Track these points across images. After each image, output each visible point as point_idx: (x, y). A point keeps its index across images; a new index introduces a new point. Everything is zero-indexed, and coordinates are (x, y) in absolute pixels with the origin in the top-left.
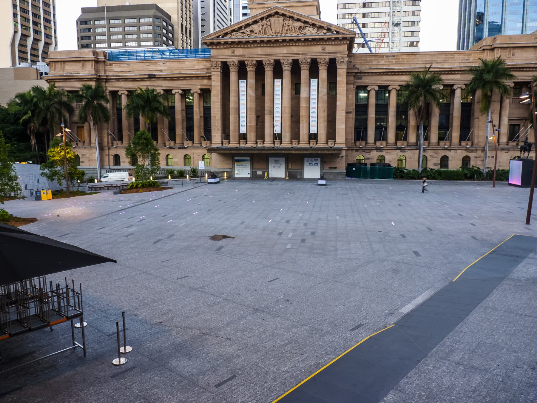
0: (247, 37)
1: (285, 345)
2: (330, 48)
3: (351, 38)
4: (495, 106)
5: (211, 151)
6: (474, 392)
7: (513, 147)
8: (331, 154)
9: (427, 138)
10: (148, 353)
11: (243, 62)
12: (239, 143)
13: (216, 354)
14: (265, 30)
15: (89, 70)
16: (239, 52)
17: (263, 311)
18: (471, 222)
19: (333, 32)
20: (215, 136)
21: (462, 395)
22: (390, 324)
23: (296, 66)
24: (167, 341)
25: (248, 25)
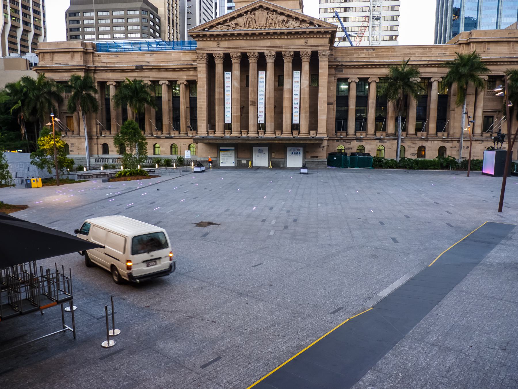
0: (232, 30)
1: (269, 327)
2: (312, 41)
3: (333, 31)
4: (470, 99)
5: (197, 140)
6: (448, 371)
7: (487, 138)
8: (313, 144)
9: (405, 129)
10: (136, 335)
12: (225, 133)
13: (201, 337)
14: (249, 23)
15: (77, 61)
16: (224, 44)
17: (247, 295)
18: (447, 210)
19: (315, 26)
20: (201, 126)
21: (437, 375)
22: (369, 308)
23: (279, 59)
24: (155, 324)
25: (233, 18)
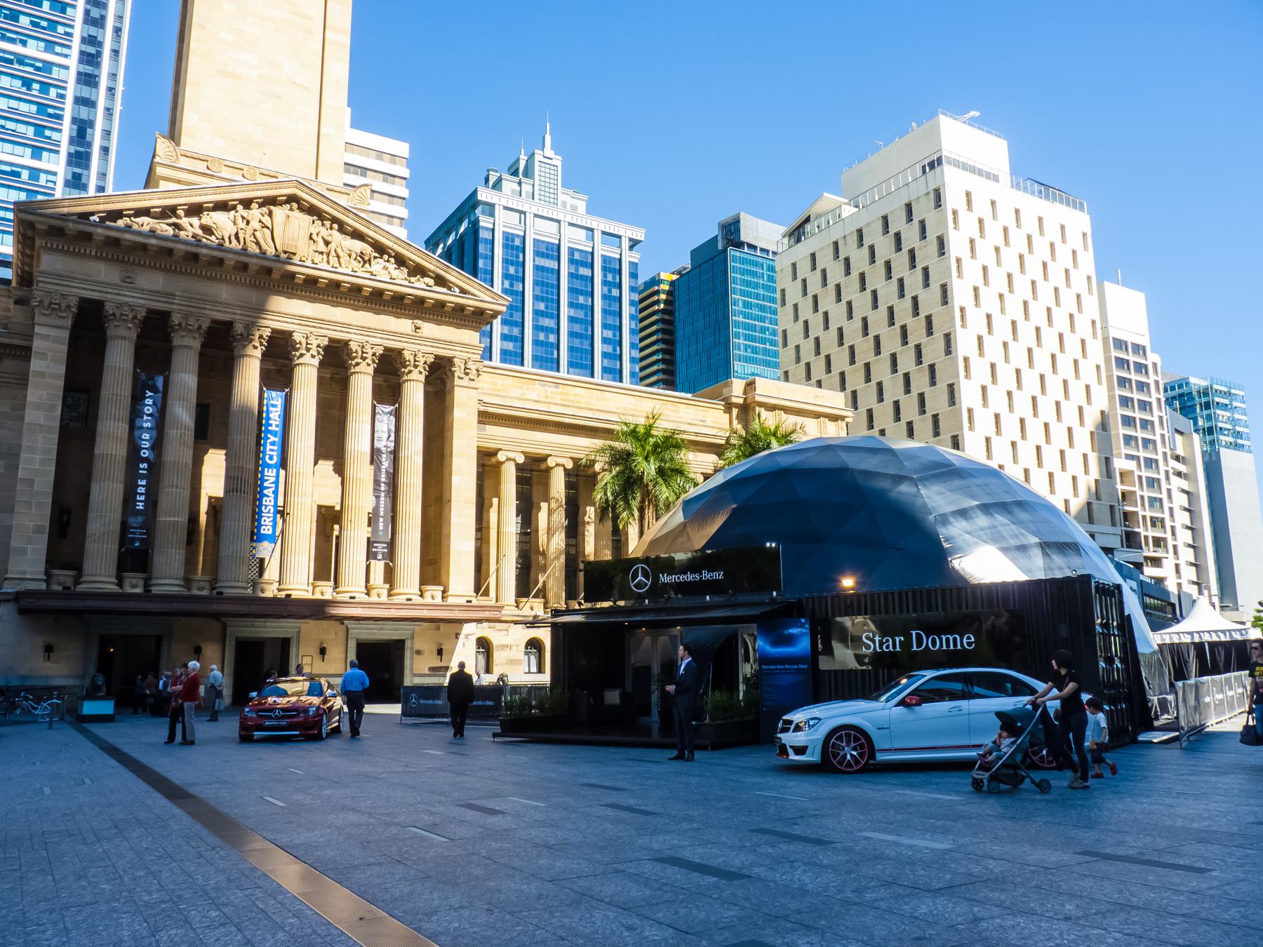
11: (166, 315)
12: (120, 584)
19: (450, 289)
20: (23, 551)
23: (336, 360)
